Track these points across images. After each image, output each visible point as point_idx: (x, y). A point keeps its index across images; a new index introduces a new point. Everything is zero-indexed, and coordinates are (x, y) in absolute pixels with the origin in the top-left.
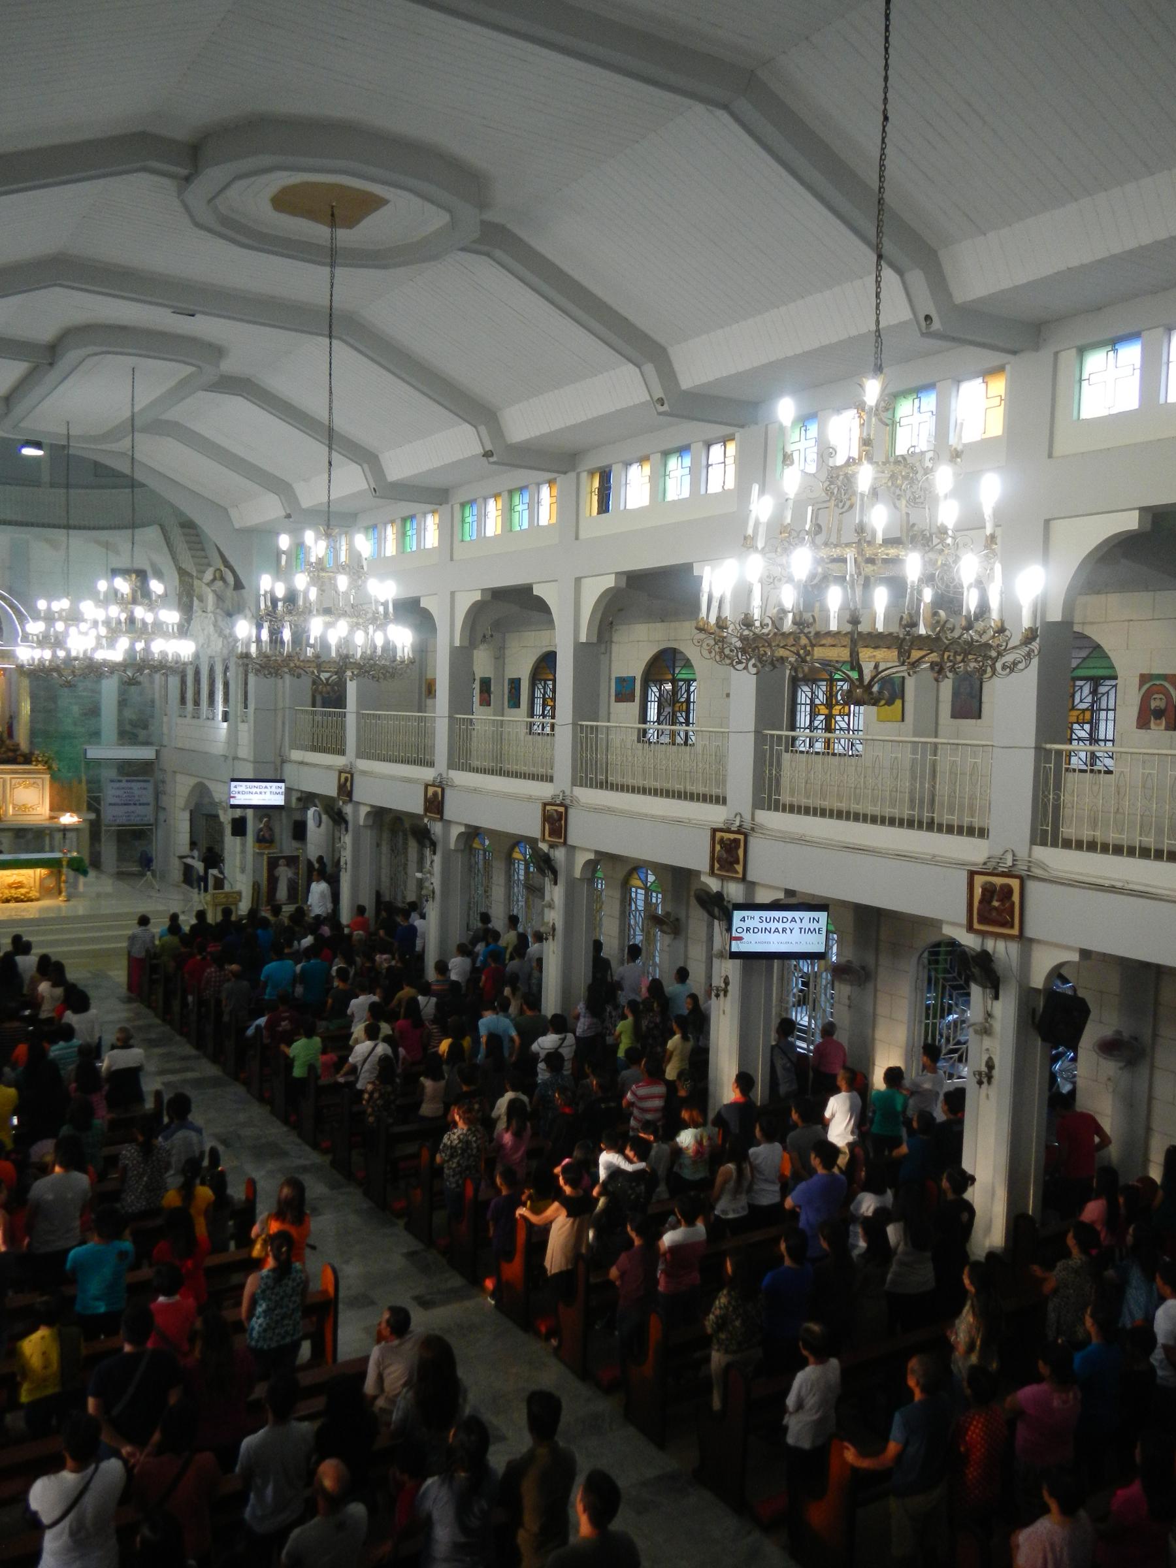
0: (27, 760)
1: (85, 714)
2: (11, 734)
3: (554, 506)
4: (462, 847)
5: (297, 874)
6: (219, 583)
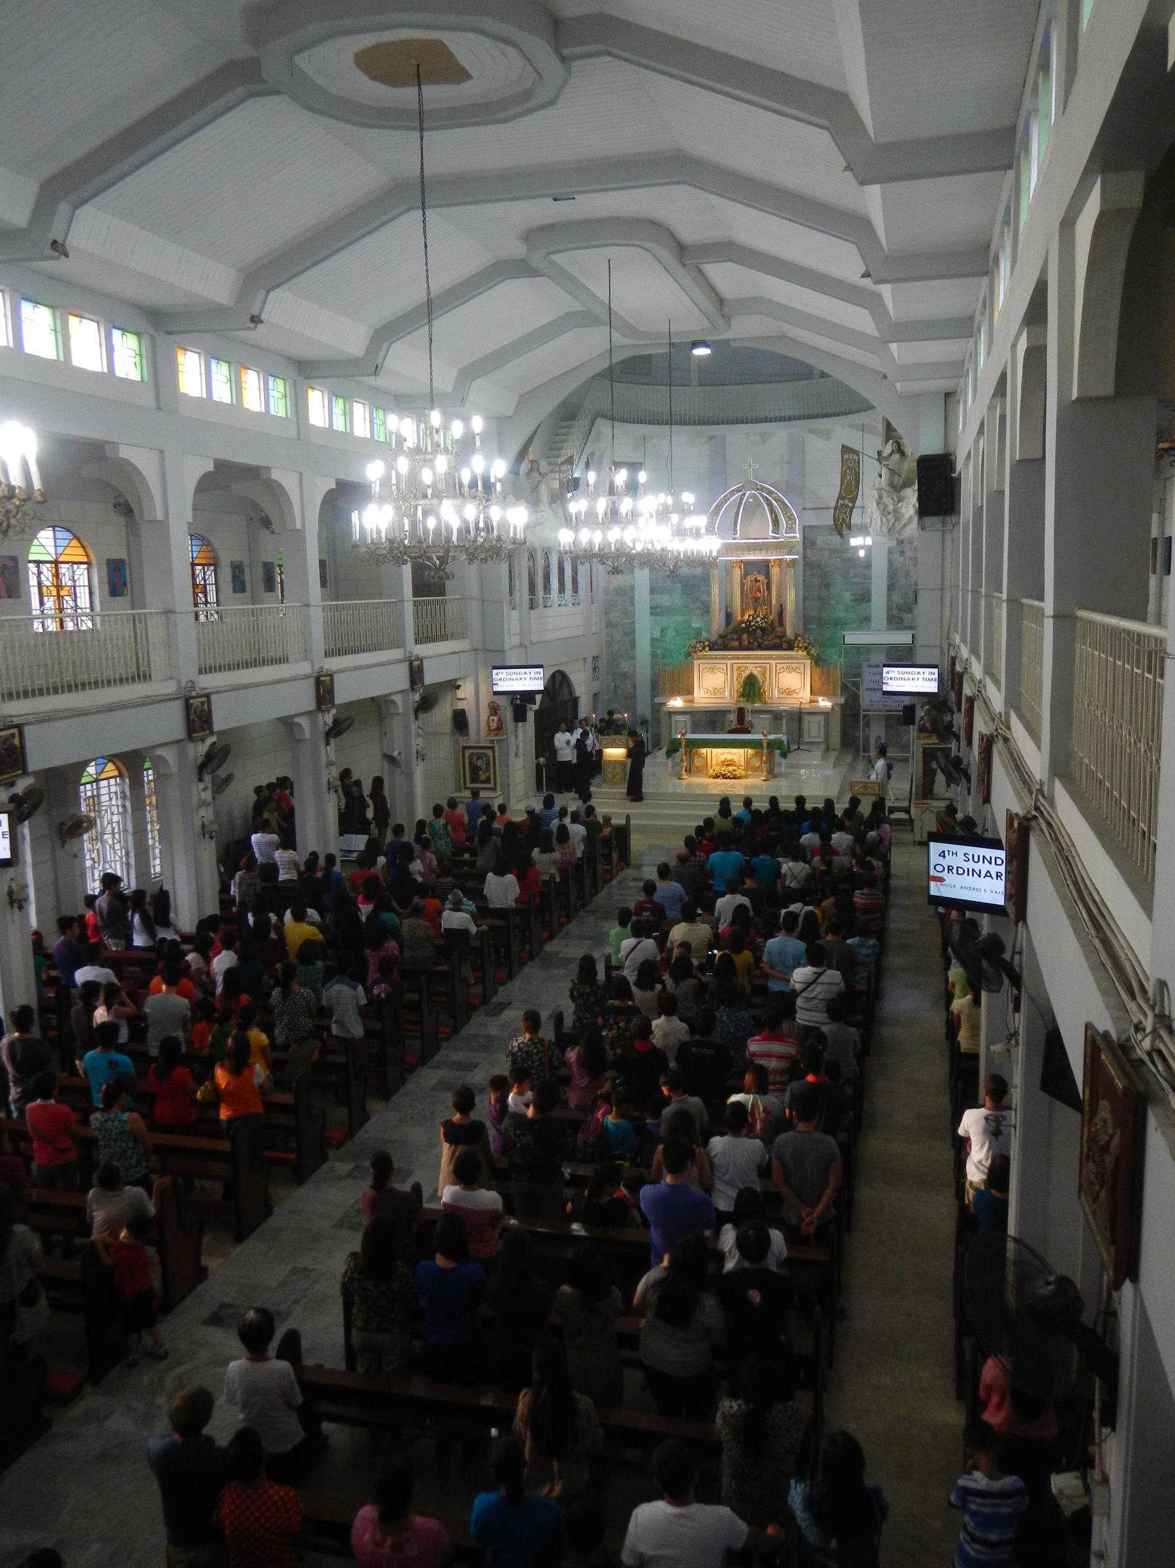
0: (791, 648)
1: (856, 600)
2: (781, 622)
6: (897, 456)
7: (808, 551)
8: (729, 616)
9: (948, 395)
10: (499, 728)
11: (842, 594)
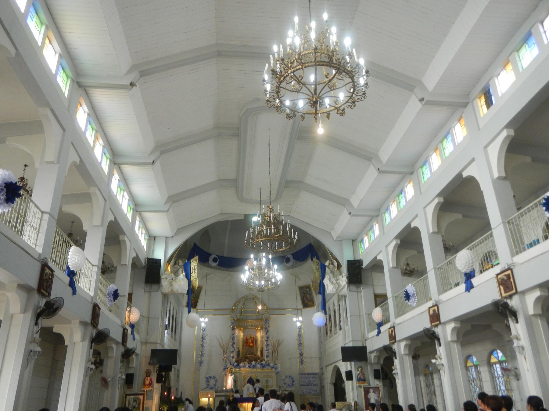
3: (465, 130)
4: (455, 339)
5: (379, 397)
6: (331, 266)
9: (353, 240)
10: (150, 384)
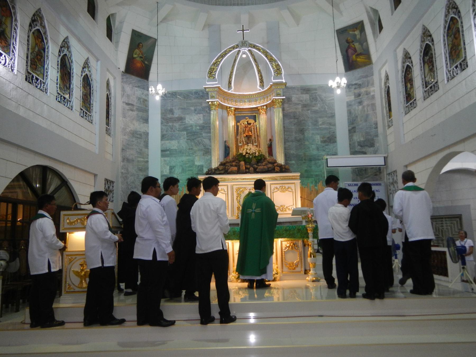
0: (283, 169)
1: (324, 142)
7: (286, 105)
8: (227, 150)
11: (315, 138)
